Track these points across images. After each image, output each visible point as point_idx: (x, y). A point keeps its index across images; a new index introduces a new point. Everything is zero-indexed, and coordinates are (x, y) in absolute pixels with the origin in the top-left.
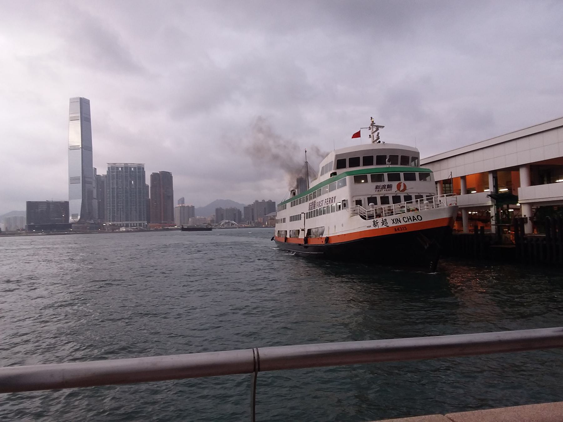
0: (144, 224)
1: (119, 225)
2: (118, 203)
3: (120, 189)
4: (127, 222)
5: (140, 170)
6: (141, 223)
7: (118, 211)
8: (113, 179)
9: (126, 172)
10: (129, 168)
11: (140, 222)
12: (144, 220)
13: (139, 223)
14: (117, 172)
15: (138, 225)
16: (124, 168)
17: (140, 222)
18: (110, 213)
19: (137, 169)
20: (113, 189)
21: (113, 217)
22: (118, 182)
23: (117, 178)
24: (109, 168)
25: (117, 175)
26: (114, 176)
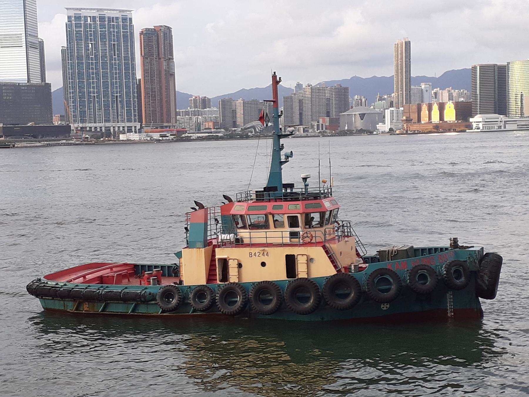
0: (135, 127)
1: (93, 130)
2: (89, 84)
3: (92, 59)
4: (107, 124)
5: (127, 21)
6: (131, 127)
7: (90, 102)
8: (79, 39)
9: (102, 26)
10: (107, 19)
11: (129, 124)
12: (135, 121)
13: (128, 127)
14: (86, 25)
15: (126, 130)
16: (98, 19)
17: (129, 124)
18: (75, 107)
19: (120, 20)
20: (80, 58)
21: (83, 114)
22: (89, 46)
23: (86, 39)
24: (69, 17)
25: (86, 32)
26: (81, 34)
